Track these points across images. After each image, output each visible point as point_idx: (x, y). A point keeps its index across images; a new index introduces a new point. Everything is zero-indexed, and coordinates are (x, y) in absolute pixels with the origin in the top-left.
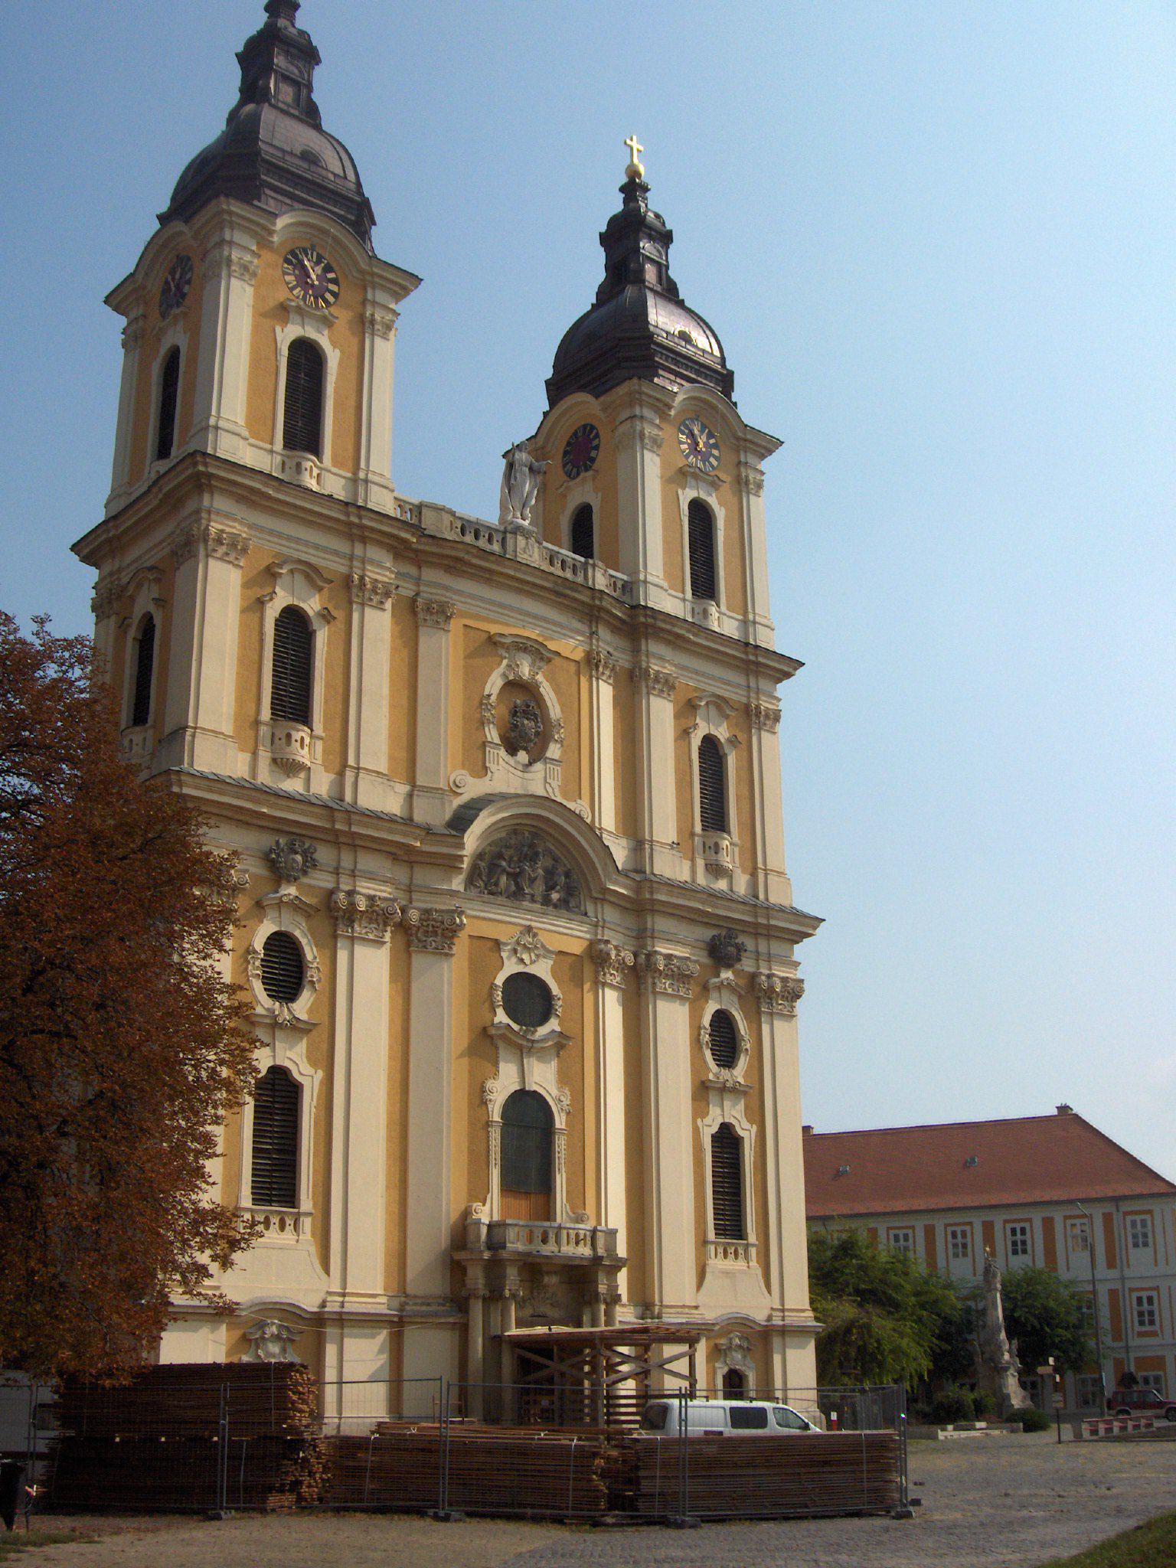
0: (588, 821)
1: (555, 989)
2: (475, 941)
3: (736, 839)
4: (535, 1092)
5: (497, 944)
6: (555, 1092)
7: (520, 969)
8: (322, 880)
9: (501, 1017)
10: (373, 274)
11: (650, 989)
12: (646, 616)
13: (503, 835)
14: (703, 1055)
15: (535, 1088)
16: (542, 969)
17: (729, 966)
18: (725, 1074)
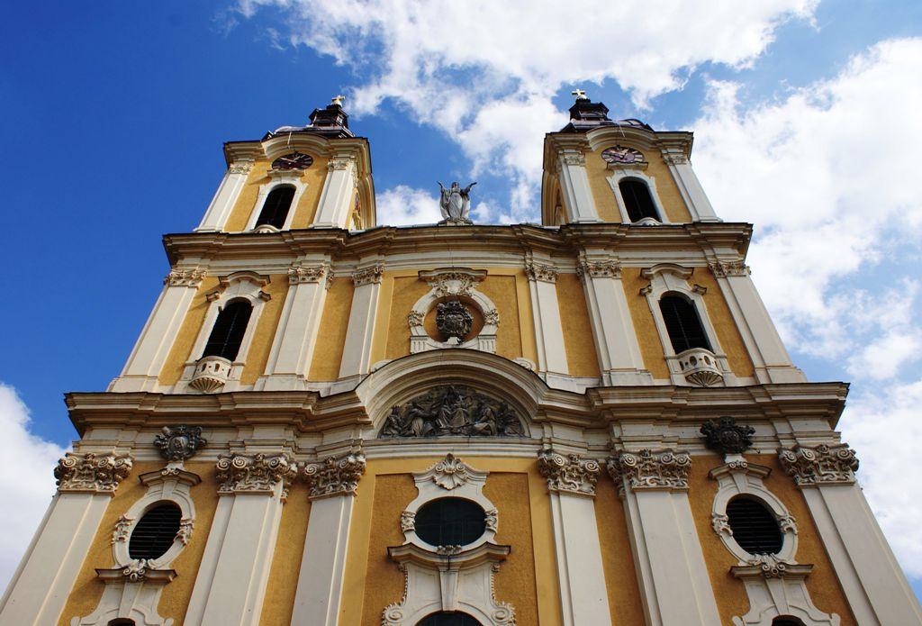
0: (534, 369)
1: (487, 505)
2: (384, 479)
3: (719, 350)
4: (457, 612)
5: (411, 476)
6: (490, 609)
7: (443, 494)
8: (210, 456)
9: (412, 538)
10: (332, 148)
11: (627, 489)
12: (571, 232)
13: (426, 392)
14: (725, 547)
15: (457, 607)
16: (472, 491)
17: (735, 451)
18: (769, 561)
